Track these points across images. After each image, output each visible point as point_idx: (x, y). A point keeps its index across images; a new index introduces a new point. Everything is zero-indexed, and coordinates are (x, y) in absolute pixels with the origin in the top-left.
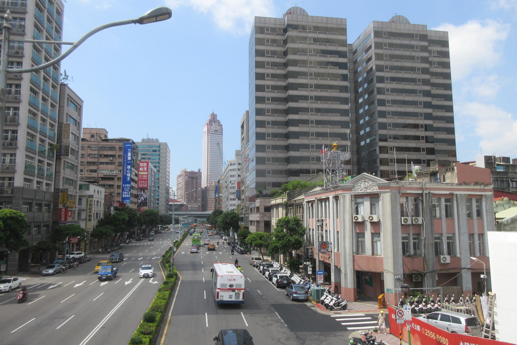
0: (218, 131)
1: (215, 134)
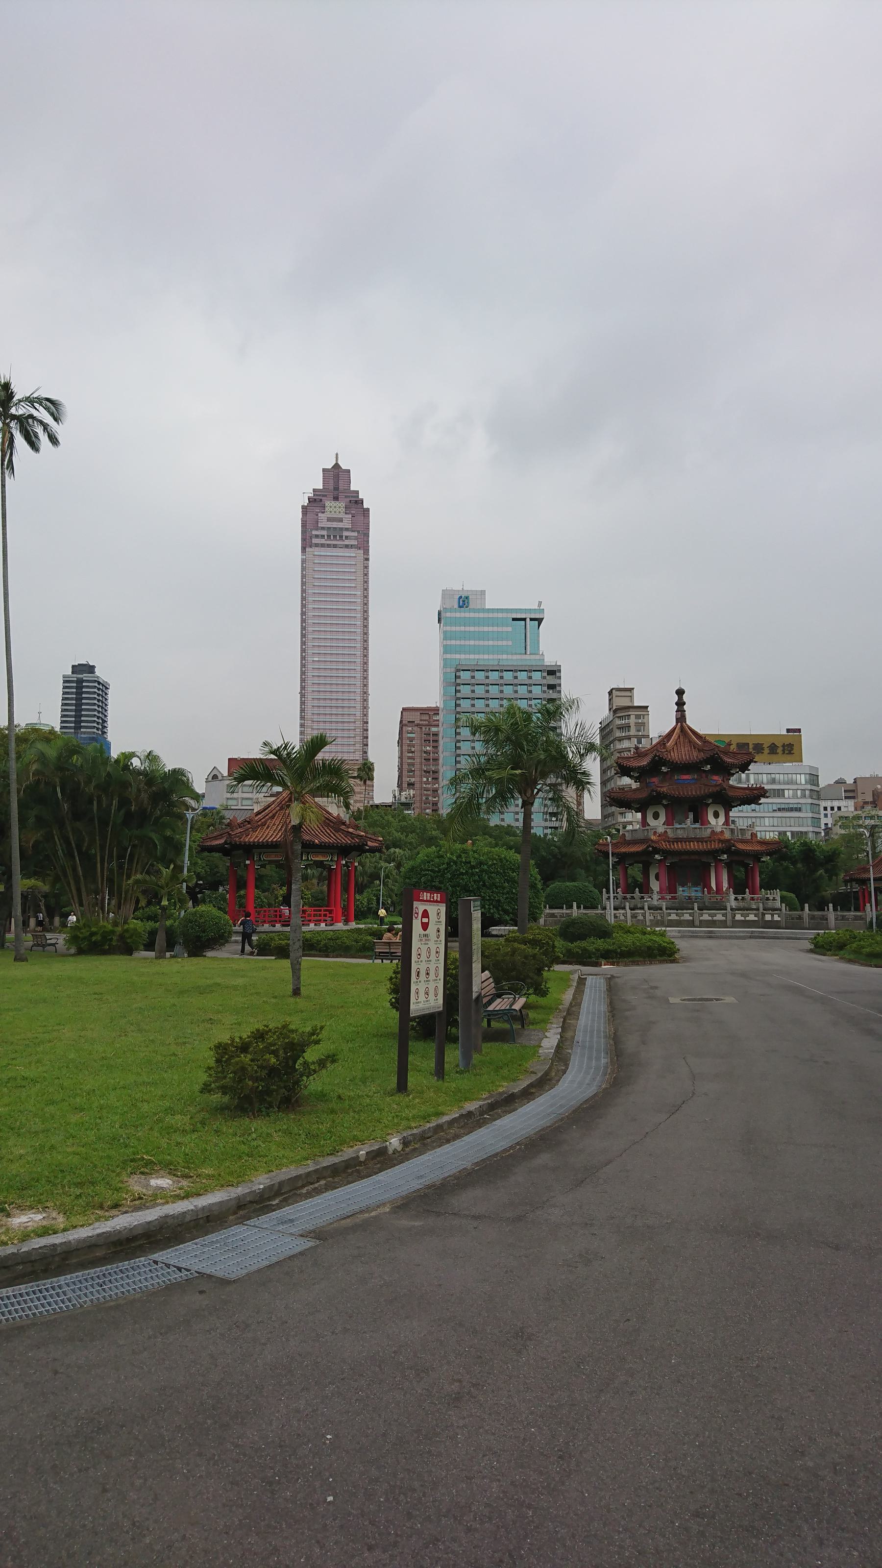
0: (345, 534)
1: (329, 546)
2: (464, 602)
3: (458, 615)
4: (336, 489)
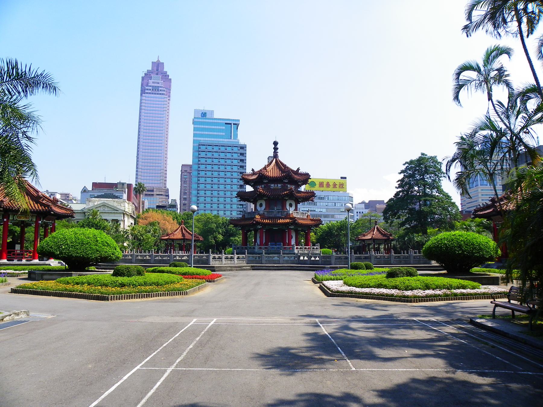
0: (160, 89)
1: (152, 93)
2: (204, 115)
3: (200, 120)
4: (157, 70)
